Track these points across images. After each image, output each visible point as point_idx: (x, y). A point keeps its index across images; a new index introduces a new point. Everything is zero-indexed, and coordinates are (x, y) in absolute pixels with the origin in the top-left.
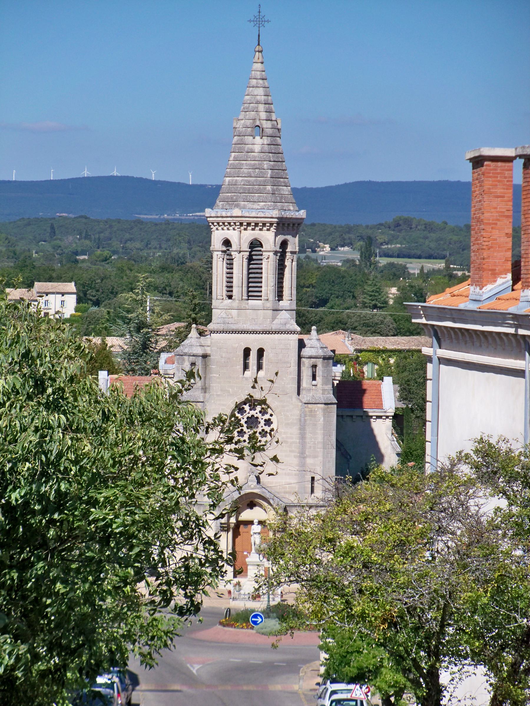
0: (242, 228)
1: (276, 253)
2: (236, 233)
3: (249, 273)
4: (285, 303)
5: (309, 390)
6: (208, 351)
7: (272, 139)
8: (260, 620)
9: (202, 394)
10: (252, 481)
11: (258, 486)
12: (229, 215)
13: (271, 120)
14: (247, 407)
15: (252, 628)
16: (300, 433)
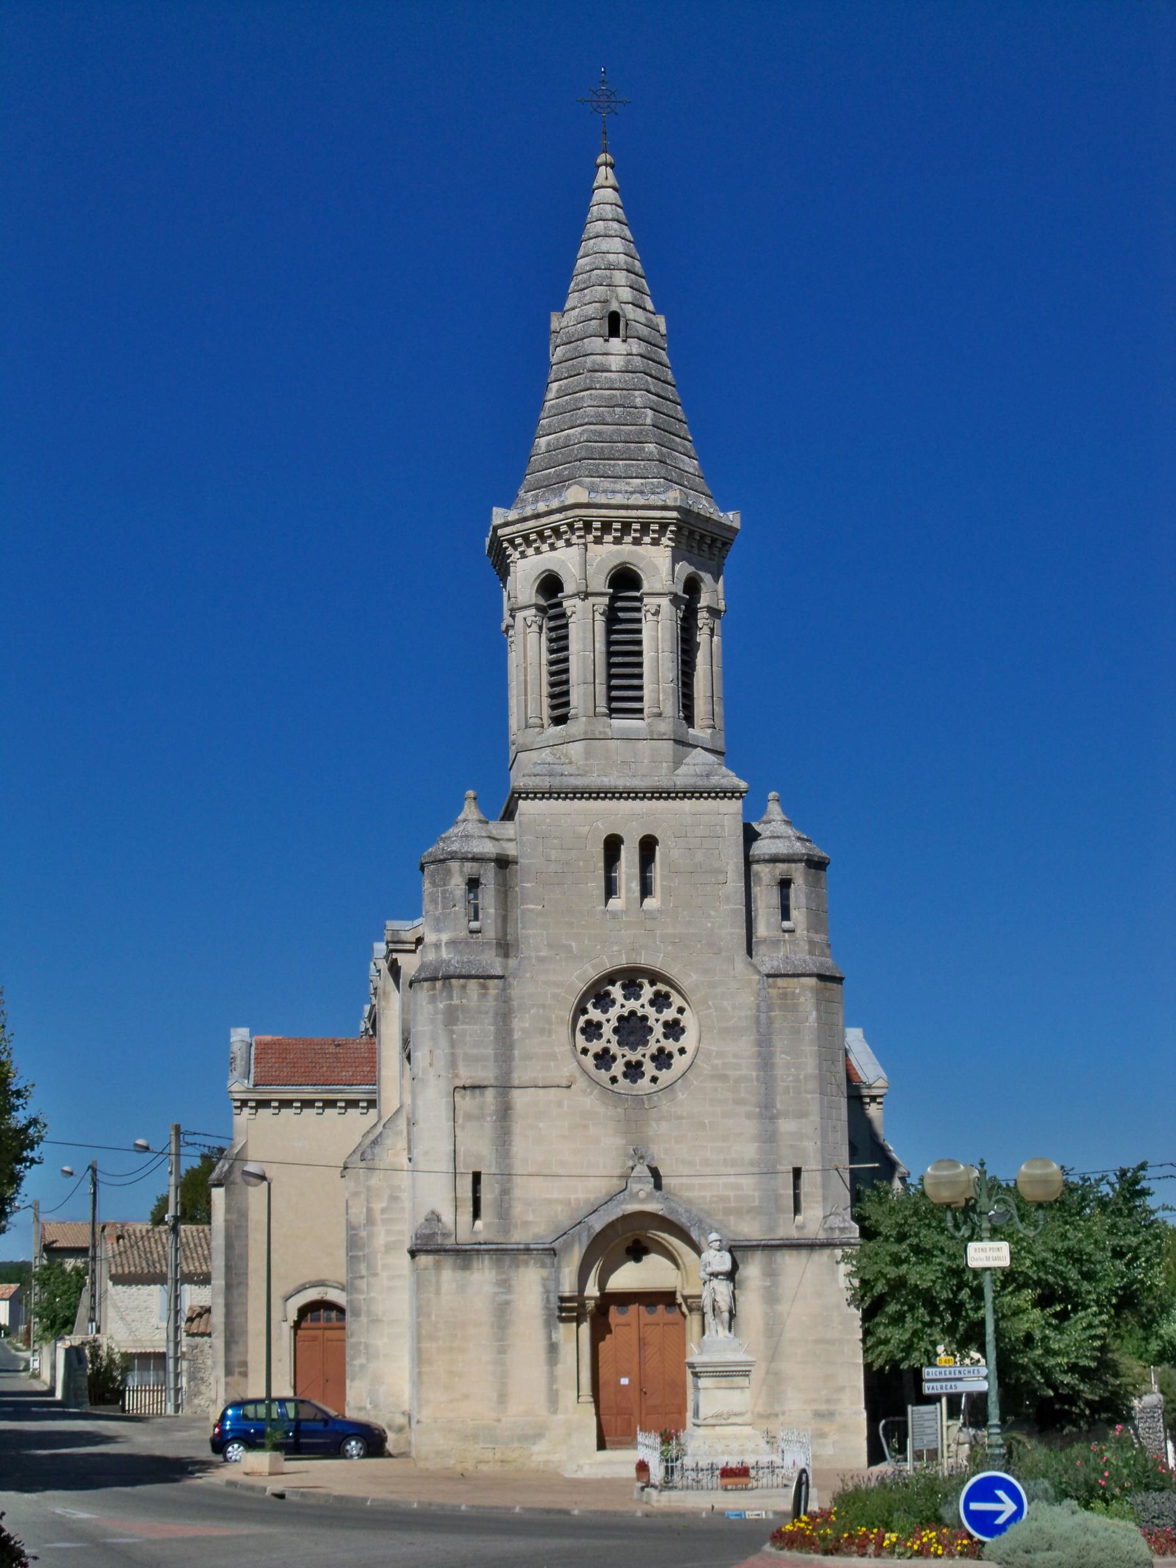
0: (590, 538)
1: (675, 600)
2: (574, 551)
3: (610, 654)
4: (700, 732)
5: (776, 943)
6: (511, 850)
7: (650, 347)
8: (1009, 1507)
9: (499, 959)
10: (639, 1179)
11: (658, 1194)
12: (555, 504)
13: (644, 309)
14: (616, 991)
15: (975, 1551)
16: (760, 1054)
